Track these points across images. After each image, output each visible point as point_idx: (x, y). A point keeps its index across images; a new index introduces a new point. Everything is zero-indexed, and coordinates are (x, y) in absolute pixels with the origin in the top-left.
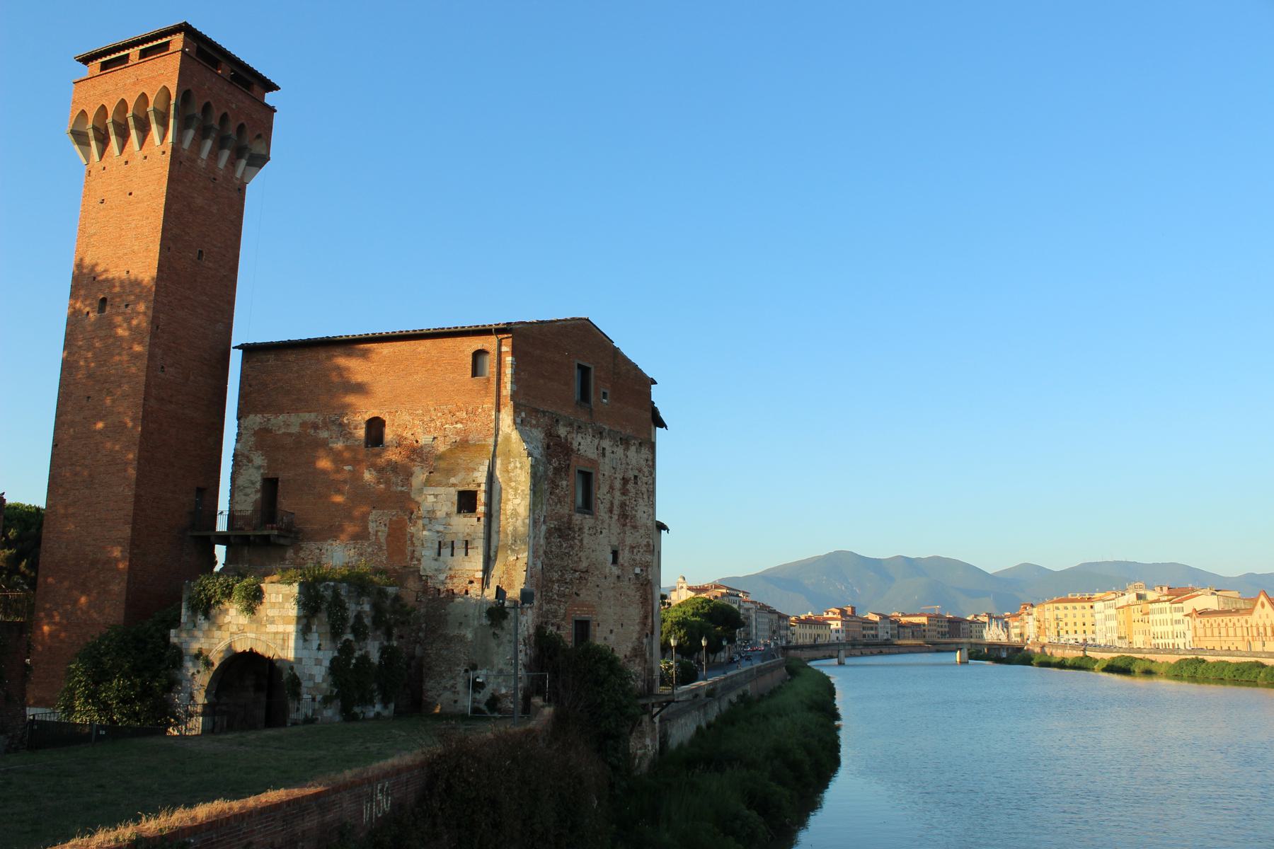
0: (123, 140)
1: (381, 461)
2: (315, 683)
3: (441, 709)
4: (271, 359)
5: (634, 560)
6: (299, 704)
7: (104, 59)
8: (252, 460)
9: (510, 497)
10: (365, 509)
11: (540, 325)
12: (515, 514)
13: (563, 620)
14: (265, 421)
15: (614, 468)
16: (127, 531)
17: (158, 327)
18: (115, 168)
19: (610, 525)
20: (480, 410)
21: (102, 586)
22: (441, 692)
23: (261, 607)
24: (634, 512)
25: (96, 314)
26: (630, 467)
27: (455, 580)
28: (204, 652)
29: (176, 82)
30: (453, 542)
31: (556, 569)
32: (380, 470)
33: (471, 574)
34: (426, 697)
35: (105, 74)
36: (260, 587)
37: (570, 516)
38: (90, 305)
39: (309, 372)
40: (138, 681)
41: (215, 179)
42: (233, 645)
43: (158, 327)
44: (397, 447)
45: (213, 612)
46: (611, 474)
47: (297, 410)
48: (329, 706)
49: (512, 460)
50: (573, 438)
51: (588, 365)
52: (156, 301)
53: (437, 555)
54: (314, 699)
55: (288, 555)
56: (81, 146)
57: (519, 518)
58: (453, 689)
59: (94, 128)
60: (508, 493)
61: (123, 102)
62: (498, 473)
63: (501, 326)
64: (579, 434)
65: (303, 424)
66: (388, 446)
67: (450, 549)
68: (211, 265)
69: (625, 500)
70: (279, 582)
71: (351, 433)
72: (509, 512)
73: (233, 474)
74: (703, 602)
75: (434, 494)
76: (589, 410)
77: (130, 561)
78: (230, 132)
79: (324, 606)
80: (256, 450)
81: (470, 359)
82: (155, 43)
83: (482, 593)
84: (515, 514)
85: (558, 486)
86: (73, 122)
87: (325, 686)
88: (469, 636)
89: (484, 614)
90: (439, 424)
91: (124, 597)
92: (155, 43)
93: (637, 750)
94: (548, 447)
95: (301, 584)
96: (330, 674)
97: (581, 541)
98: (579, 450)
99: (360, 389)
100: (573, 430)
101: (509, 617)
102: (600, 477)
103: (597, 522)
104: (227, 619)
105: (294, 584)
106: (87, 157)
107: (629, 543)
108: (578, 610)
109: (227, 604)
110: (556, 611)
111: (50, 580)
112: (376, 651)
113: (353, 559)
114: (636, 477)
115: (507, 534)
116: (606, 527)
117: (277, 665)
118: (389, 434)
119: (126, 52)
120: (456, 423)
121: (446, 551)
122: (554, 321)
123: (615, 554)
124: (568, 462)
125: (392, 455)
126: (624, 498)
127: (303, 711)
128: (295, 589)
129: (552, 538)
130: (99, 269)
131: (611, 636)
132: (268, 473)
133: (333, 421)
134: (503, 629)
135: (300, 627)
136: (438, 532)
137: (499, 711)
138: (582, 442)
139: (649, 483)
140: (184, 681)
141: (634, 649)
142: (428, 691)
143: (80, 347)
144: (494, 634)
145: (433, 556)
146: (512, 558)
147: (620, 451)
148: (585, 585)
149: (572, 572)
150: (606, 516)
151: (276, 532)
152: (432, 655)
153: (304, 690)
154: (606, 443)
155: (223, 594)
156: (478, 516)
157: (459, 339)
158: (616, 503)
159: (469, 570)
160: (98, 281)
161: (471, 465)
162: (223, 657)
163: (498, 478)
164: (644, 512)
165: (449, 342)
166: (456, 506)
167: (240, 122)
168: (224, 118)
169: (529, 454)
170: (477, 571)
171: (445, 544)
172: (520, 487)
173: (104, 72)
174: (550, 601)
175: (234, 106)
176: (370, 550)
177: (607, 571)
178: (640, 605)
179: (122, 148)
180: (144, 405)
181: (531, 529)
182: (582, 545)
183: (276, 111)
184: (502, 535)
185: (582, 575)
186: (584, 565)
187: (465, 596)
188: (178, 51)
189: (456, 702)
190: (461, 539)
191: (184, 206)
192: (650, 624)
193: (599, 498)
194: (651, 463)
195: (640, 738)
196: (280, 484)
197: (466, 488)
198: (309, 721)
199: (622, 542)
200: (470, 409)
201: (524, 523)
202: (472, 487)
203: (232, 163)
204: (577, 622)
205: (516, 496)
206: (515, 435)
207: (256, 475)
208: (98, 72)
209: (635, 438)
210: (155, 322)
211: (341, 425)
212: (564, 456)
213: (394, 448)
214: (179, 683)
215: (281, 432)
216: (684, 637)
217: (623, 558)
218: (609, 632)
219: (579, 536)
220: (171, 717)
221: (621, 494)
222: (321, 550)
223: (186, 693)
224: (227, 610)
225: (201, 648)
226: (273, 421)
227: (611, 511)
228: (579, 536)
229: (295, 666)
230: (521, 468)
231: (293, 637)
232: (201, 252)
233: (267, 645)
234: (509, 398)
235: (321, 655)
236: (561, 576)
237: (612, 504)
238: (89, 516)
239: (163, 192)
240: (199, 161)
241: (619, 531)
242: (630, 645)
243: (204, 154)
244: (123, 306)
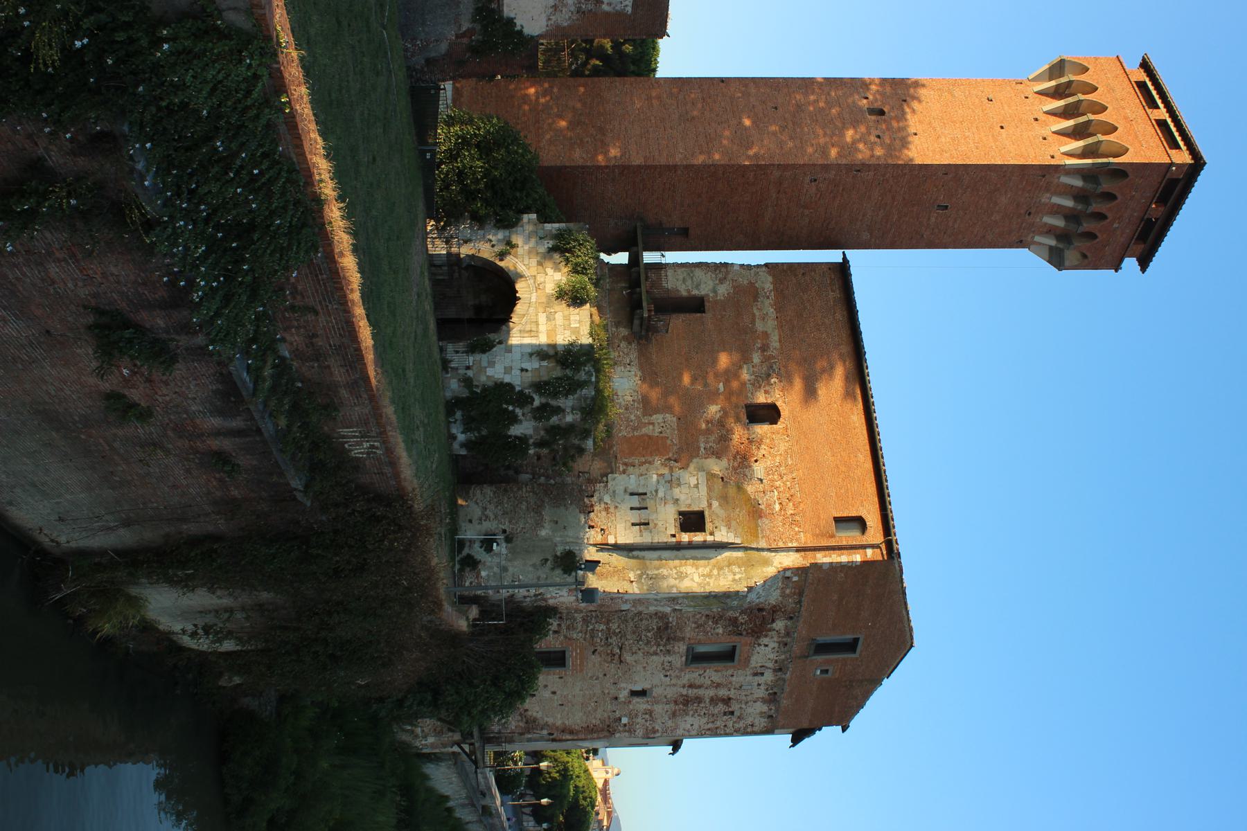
0: (1061, 114)
1: (731, 422)
2: (486, 368)
3: (462, 505)
4: (835, 294)
5: (636, 715)
6: (462, 353)
7: (1149, 84)
8: (722, 283)
9: (701, 570)
10: (677, 409)
11: (901, 591)
12: (681, 576)
13: (566, 637)
14: (766, 293)
15: (741, 687)
16: (637, 161)
17: (859, 171)
18: (1028, 108)
19: (674, 685)
20: (797, 529)
21: (578, 141)
22: (481, 505)
23: (564, 305)
24: (691, 713)
25: (866, 106)
26: (743, 706)
27: (604, 513)
28: (515, 249)
29: (1135, 162)
30: (646, 508)
32: (721, 423)
33: (612, 530)
34: (474, 489)
35: (1133, 87)
36: (586, 303)
37: (683, 639)
38: (876, 100)
39: (824, 336)
40: (482, 186)
41: (1030, 214)
42: (523, 279)
43: (859, 171)
44: (748, 439)
45: (557, 256)
46: (734, 683)
47: (780, 327)
48: (463, 384)
49: (743, 569)
50: (772, 637)
51: (858, 650)
52: (887, 166)
53: (632, 491)
54: (468, 368)
55: (621, 329)
56: (1048, 70)
57: (678, 581)
58: (484, 518)
59: (1070, 83)
60: (705, 566)
61: (1104, 109)
62: (727, 554)
63: (895, 546)
64: (778, 644)
65: (766, 335)
66: (748, 429)
67: (638, 506)
68: (933, 220)
69: (705, 702)
70: (592, 322)
71: (760, 387)
72: (683, 569)
73: (706, 264)
74: (591, 798)
75: (698, 483)
76: (806, 654)
77: (607, 167)
78: (1085, 225)
79: (569, 372)
80: (734, 287)
81: (854, 514)
82: (1176, 134)
83: (591, 545)
84: (681, 576)
85: (717, 623)
86: (1074, 60)
87: (483, 379)
88: (543, 533)
89: (567, 548)
90: (778, 484)
91: (567, 164)
92: (1176, 134)
93: (421, 727)
94: (760, 610)
95: (591, 346)
96: (496, 384)
97: (655, 653)
98: (759, 645)
99: (810, 393)
101: (566, 576)
102: (730, 672)
103: (677, 671)
104: (550, 271)
105: (591, 338)
106: (1037, 79)
107: (656, 709)
108: (576, 653)
109: (566, 270)
110: (574, 629)
111: (582, 89)
112: (522, 431)
113: (621, 400)
114: (732, 713)
115: (658, 569)
117: (504, 327)
118: (762, 429)
119: (1161, 106)
120: (780, 503)
121: (635, 501)
122: (906, 608)
123: (643, 693)
124: (744, 633)
125: (739, 434)
126: (708, 700)
127: (456, 357)
128: (586, 340)
129: (657, 620)
130: (915, 105)
132: (709, 302)
133: (771, 367)
134: (553, 569)
135: (545, 349)
136: (656, 491)
137: (461, 570)
139: (726, 729)
140: (483, 232)
141: (535, 720)
142: (482, 490)
143: (829, 94)
144: (547, 560)
145: (630, 487)
146: (632, 576)
147: (761, 693)
148: (605, 661)
149: (620, 644)
150: (685, 681)
151: (646, 315)
152: (520, 492)
153: (478, 356)
154: (769, 676)
155: (577, 264)
156: (677, 535)
157: (876, 499)
158: (701, 692)
159: (616, 528)
160: (902, 104)
161: (734, 523)
162: (509, 270)
163: (720, 554)
164: (692, 725)
165: (872, 488)
166: (687, 509)
167: (1098, 234)
168: (1100, 216)
169: (750, 589)
170: (616, 538)
171: (643, 499)
172: (713, 579)
173: (1135, 86)
174: (586, 621)
175: (1116, 225)
176: (633, 417)
177: (623, 685)
178: (584, 725)
179: (1052, 113)
180: (773, 165)
181: (666, 596)
182: (652, 655)
183: (1116, 271)
184: (656, 563)
185: (617, 656)
186: (628, 658)
187: (587, 526)
188: (1170, 159)
189: (470, 521)
190: (650, 518)
191: (996, 184)
192: (564, 738)
193: (705, 672)
194: (749, 730)
195: (435, 730)
196: (699, 315)
197: (707, 520)
198: (445, 364)
199: (657, 702)
200: (797, 518)
201: (673, 587)
202: (709, 526)
203: (1050, 231)
204: (564, 652)
205: (702, 576)
206: (771, 571)
207: (707, 290)
208: (1134, 79)
209: (777, 710)
210: (863, 167)
211: (768, 376)
212: (751, 628)
213: (746, 436)
214: (481, 227)
215: (755, 311)
216: (550, 777)
217: (638, 703)
218: (553, 690)
219: (661, 650)
220: (445, 222)
221: (712, 697)
222: (629, 365)
223: (471, 236)
224: (559, 270)
225: (518, 247)
226: (767, 302)
227: (691, 686)
228: (661, 650)
229: (502, 346)
230: (734, 580)
231: (534, 341)
232: (946, 207)
233: (524, 315)
234: (813, 562)
235: (516, 372)
236: (614, 633)
237: (700, 687)
238: (651, 121)
239: (1009, 161)
240: (1048, 195)
241: (668, 697)
242: (539, 715)
243: (1056, 200)
244: (878, 133)
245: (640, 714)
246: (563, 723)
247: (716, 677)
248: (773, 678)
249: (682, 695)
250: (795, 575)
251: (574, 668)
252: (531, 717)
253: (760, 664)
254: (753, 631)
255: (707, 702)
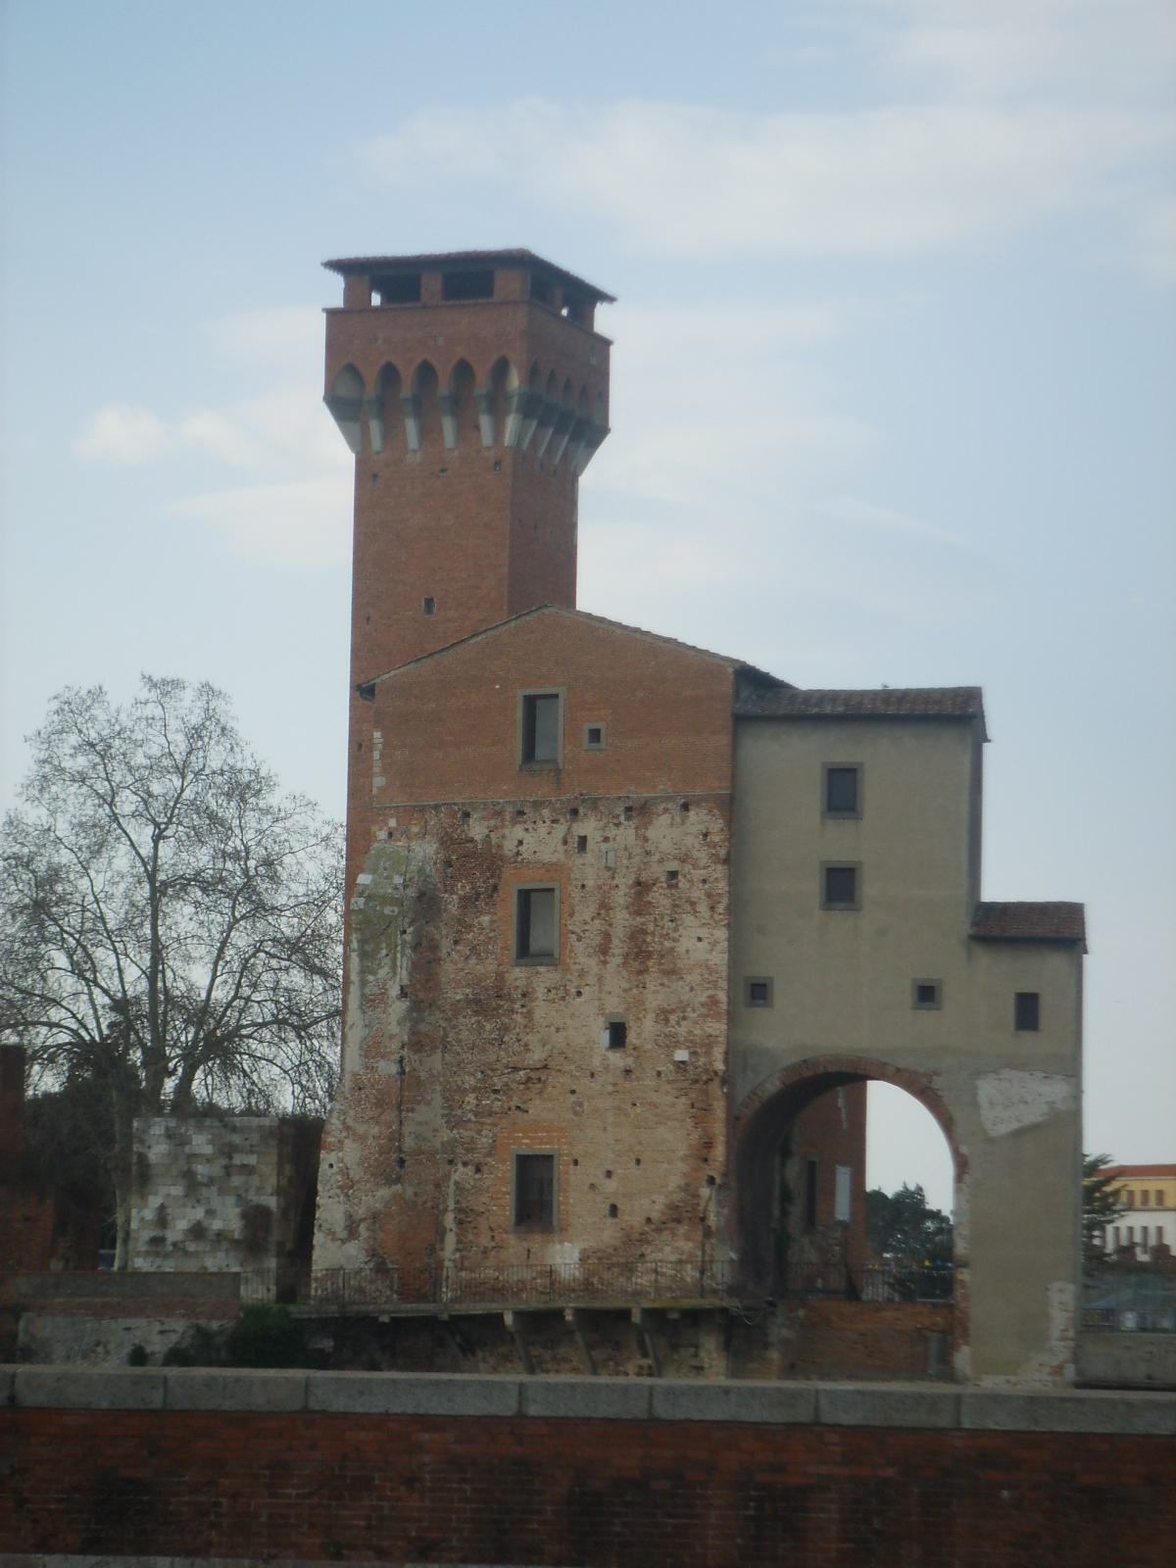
13: (489, 1155)
15: (608, 868)
19: (600, 979)
24: (668, 944)
31: (470, 1068)
37: (500, 976)
46: (600, 882)
50: (503, 837)
69: (643, 924)
94: (448, 863)
97: (529, 1015)
98: (518, 854)
100: (503, 820)
102: (576, 893)
107: (655, 1004)
108: (523, 1138)
110: (472, 1140)
116: (592, 980)
129: (460, 1017)
131: (607, 1182)
138: (528, 839)
141: (673, 1207)
147: (626, 834)
148: (540, 1093)
149: (506, 1071)
150: (592, 964)
154: (588, 827)
158: (619, 933)
177: (596, 1062)
185: (533, 1075)
186: (537, 1056)
199: (639, 1004)
209: (669, 799)
221: (630, 914)
227: (604, 950)
228: (523, 1006)
232: (429, 602)
236: (483, 1080)
237: (607, 936)
241: (626, 985)
242: (661, 1201)
245: (667, 1030)
246: (682, 1160)
247: (585, 912)
248: (593, 819)
249: (625, 964)
250: (386, 824)
251: (556, 1141)
252: (664, 1213)
253: (561, 848)
254: (488, 869)
255: (643, 920)
